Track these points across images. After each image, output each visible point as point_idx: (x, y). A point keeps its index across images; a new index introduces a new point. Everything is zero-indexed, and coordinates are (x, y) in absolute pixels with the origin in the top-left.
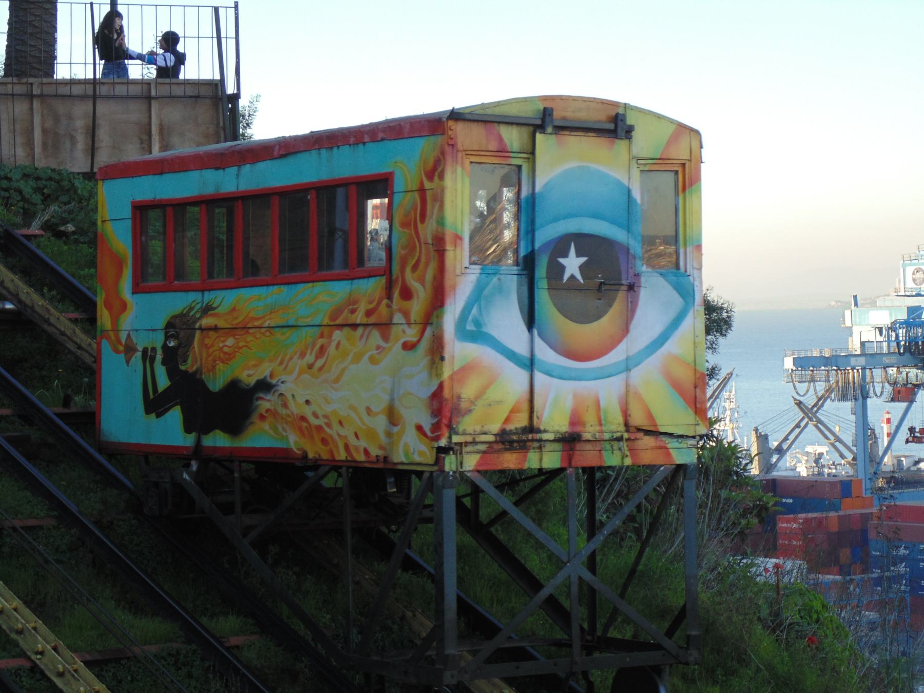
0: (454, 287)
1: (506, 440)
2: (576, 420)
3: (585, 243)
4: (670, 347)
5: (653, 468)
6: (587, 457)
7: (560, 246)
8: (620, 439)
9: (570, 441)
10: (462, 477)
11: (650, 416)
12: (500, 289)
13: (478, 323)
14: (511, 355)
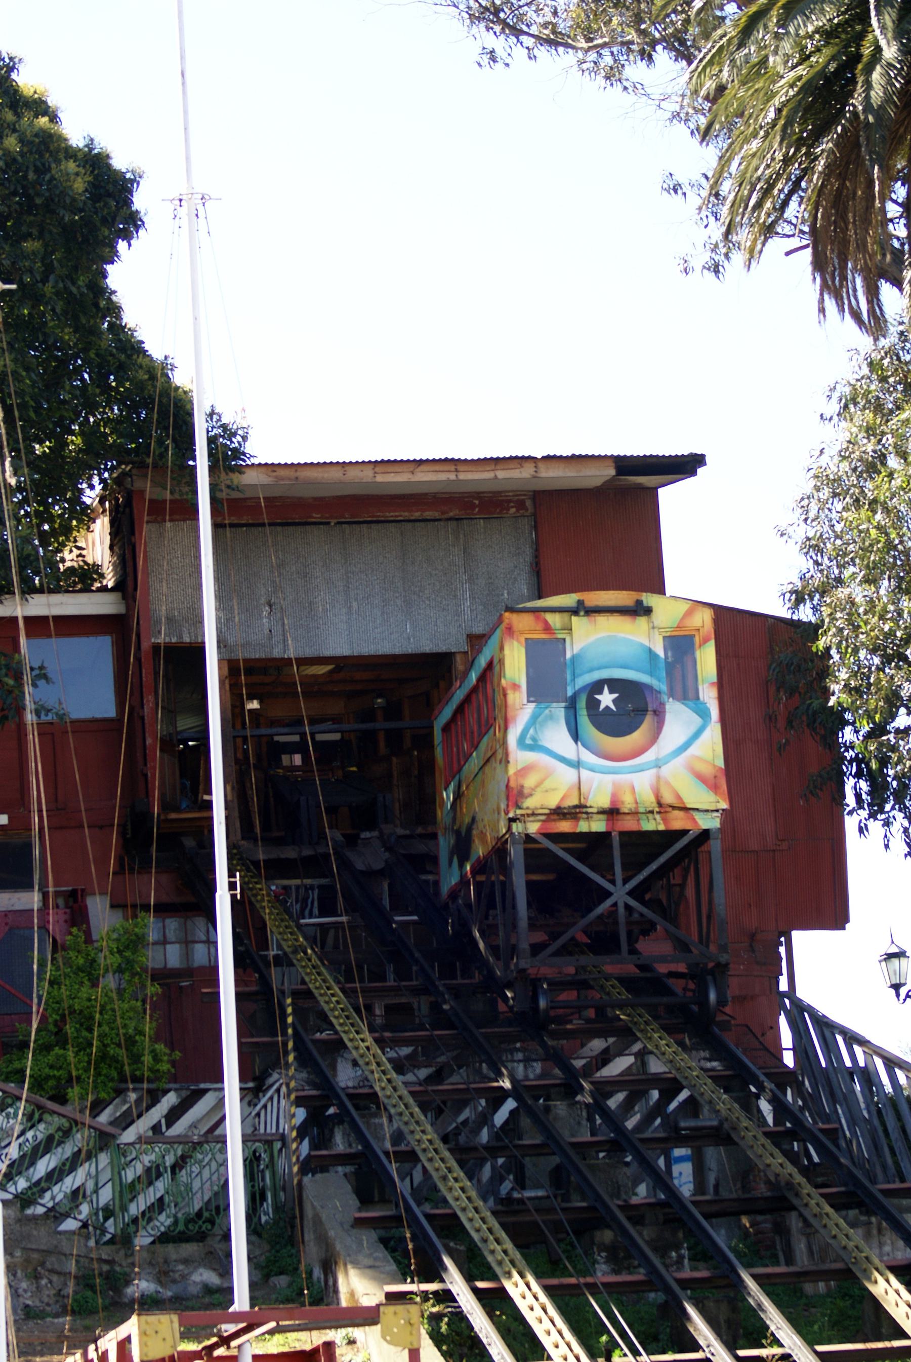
0: (514, 718)
1: (559, 813)
2: (615, 799)
3: (614, 684)
4: (693, 750)
5: (685, 832)
6: (629, 824)
7: (597, 687)
8: (652, 812)
9: (612, 813)
10: (528, 838)
11: (679, 797)
12: (551, 717)
13: (534, 739)
14: (562, 759)
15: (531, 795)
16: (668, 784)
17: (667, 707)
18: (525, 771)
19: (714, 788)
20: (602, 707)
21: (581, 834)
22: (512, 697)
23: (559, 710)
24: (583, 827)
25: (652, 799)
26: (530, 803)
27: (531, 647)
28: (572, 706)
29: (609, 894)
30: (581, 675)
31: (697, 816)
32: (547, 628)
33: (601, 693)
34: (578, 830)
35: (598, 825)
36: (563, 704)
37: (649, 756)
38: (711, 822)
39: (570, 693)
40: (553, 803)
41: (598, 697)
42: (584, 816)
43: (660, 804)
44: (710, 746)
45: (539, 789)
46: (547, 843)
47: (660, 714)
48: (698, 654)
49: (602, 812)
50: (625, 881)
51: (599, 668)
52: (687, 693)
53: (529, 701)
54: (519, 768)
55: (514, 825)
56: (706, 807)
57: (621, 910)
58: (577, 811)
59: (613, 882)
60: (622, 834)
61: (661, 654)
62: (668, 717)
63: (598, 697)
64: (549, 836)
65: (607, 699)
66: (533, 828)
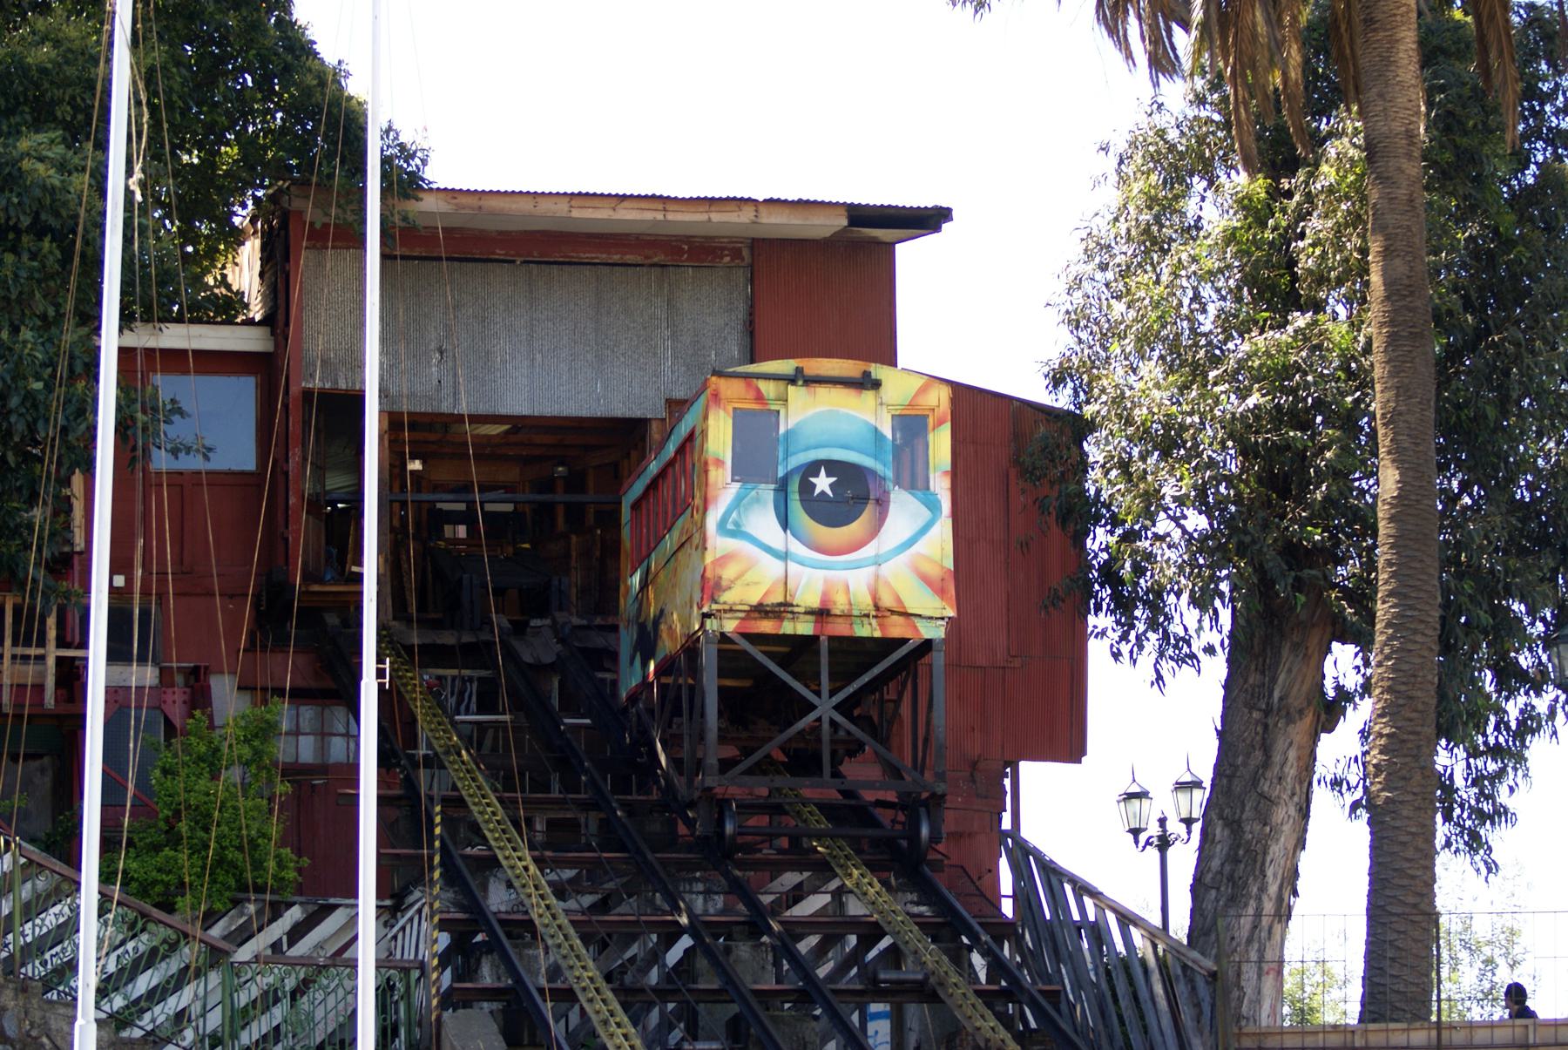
0: (716, 498)
1: (760, 610)
2: (825, 598)
3: (832, 467)
5: (904, 641)
6: (839, 628)
7: (813, 468)
8: (867, 616)
9: (822, 614)
10: (724, 637)
11: (899, 600)
12: (757, 500)
13: (737, 524)
14: (768, 549)
16: (887, 584)
17: (892, 496)
18: (723, 560)
19: (941, 592)
20: (817, 491)
21: (786, 637)
22: (713, 474)
23: (767, 493)
24: (788, 628)
25: (869, 601)
26: (728, 597)
27: (739, 417)
28: (782, 487)
29: (813, 707)
31: (920, 624)
32: (759, 397)
33: (817, 475)
35: (805, 628)
37: (868, 551)
38: (934, 632)
39: (781, 474)
40: (754, 600)
41: (813, 480)
43: (877, 608)
44: (939, 544)
45: (739, 582)
46: (745, 645)
47: (882, 504)
48: (931, 437)
49: (809, 612)
50: (832, 693)
51: (816, 447)
52: (916, 482)
55: (708, 622)
56: (929, 612)
57: (826, 726)
58: (781, 610)
59: (818, 693)
60: (831, 638)
61: (888, 434)
62: (892, 508)
63: (813, 480)
65: (823, 483)
66: (730, 626)
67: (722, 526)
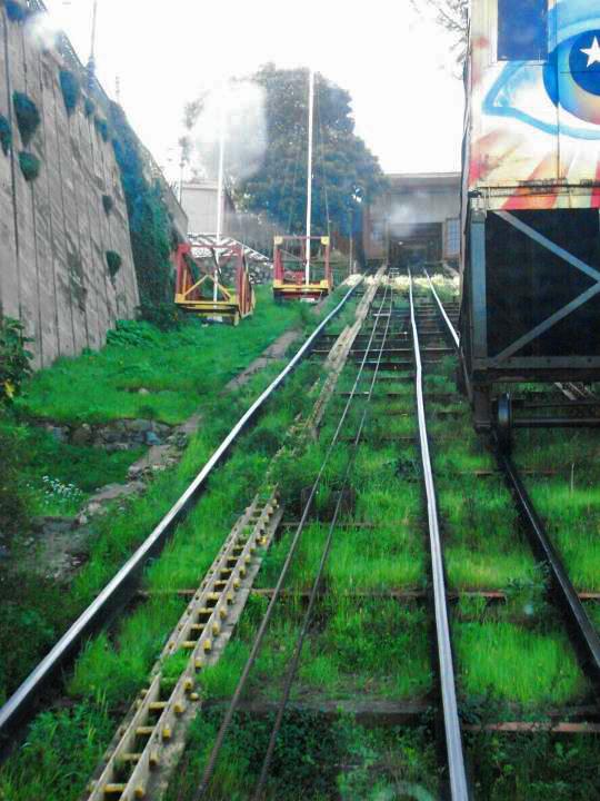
1: (529, 187)
10: (491, 217)
12: (526, 76)
13: (505, 103)
15: (498, 166)
23: (536, 68)
24: (563, 202)
26: (494, 177)
30: (565, 26)
33: (589, 46)
34: (555, 207)
35: (580, 201)
36: (542, 62)
39: (550, 49)
40: (525, 175)
41: (585, 51)
42: (564, 189)
45: (507, 160)
49: (586, 185)
53: (499, 59)
54: (484, 134)
55: (474, 201)
63: (585, 51)
64: (528, 216)
66: (498, 204)
67: (488, 105)
